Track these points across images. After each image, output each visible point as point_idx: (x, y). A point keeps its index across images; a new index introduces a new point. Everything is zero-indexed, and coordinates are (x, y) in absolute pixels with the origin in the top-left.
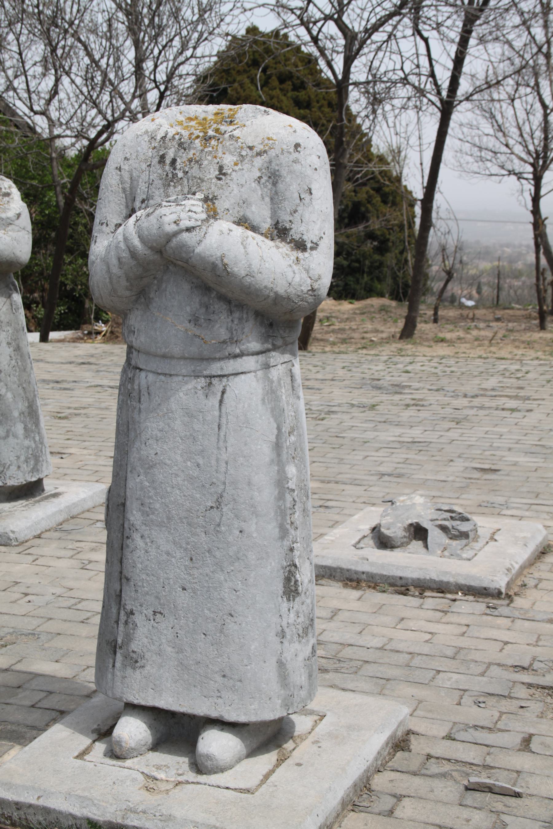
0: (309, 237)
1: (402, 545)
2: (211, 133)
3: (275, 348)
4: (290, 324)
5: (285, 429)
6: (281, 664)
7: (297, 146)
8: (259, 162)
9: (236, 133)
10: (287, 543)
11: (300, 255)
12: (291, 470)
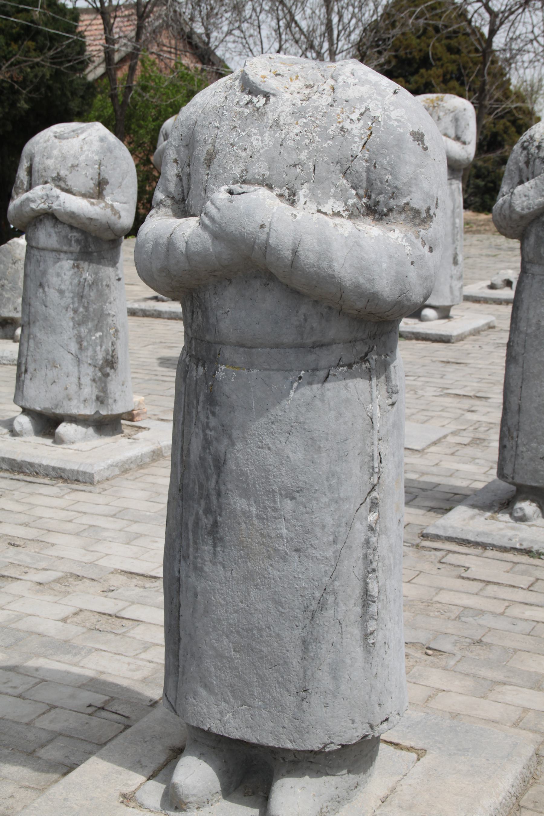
0: (467, 140)
1: (500, 288)
2: (436, 105)
3: (454, 178)
4: (459, 170)
5: (456, 206)
6: (451, 287)
7: (465, 109)
8: (452, 115)
9: (445, 105)
10: (455, 246)
11: (464, 146)
12: (457, 221)
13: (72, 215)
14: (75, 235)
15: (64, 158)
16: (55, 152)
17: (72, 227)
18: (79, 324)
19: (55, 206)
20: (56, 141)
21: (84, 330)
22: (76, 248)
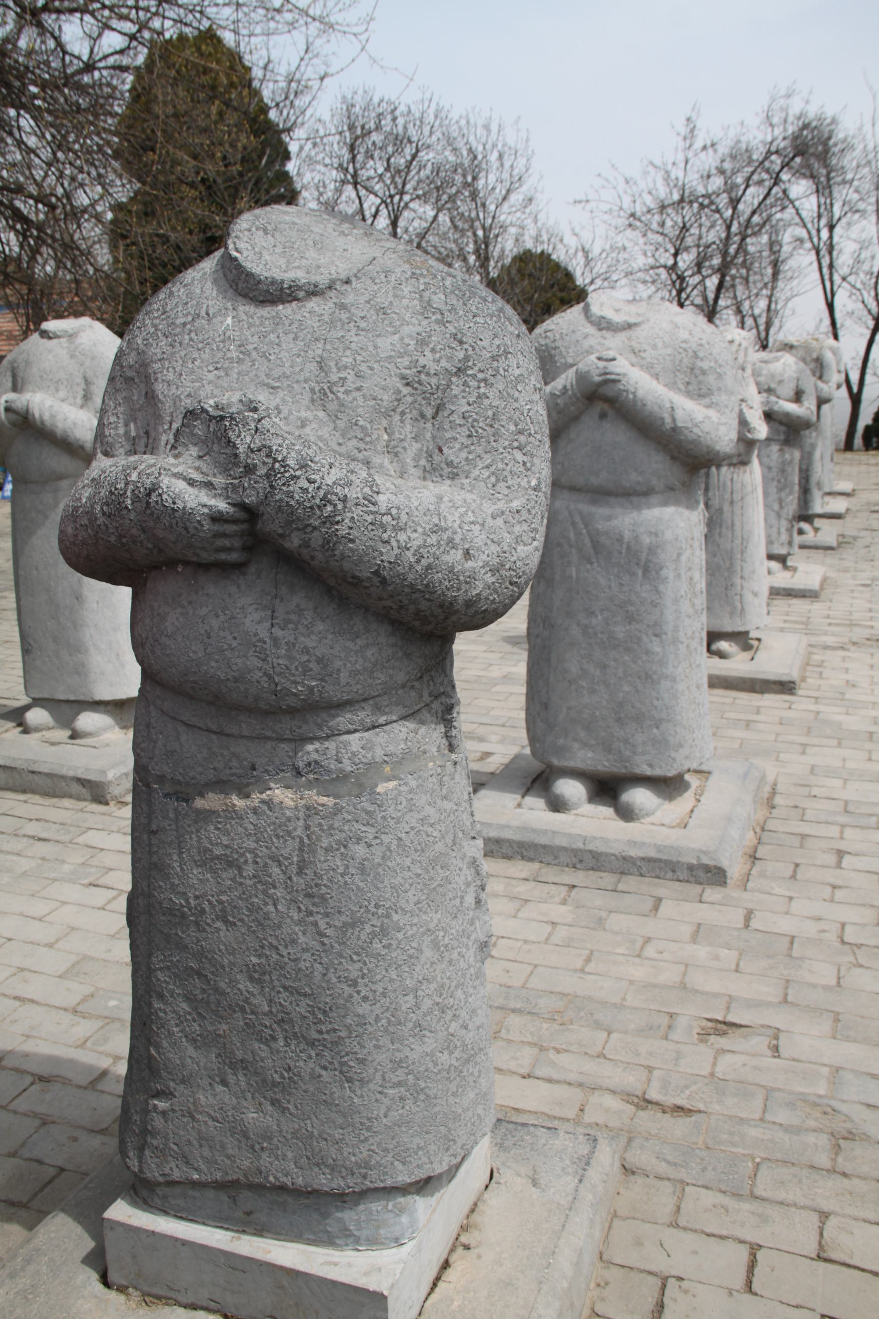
13: (787, 415)
14: (783, 428)
15: (773, 376)
16: (764, 372)
17: (781, 423)
18: (780, 490)
19: (776, 408)
20: (763, 365)
21: (783, 494)
22: (782, 437)
